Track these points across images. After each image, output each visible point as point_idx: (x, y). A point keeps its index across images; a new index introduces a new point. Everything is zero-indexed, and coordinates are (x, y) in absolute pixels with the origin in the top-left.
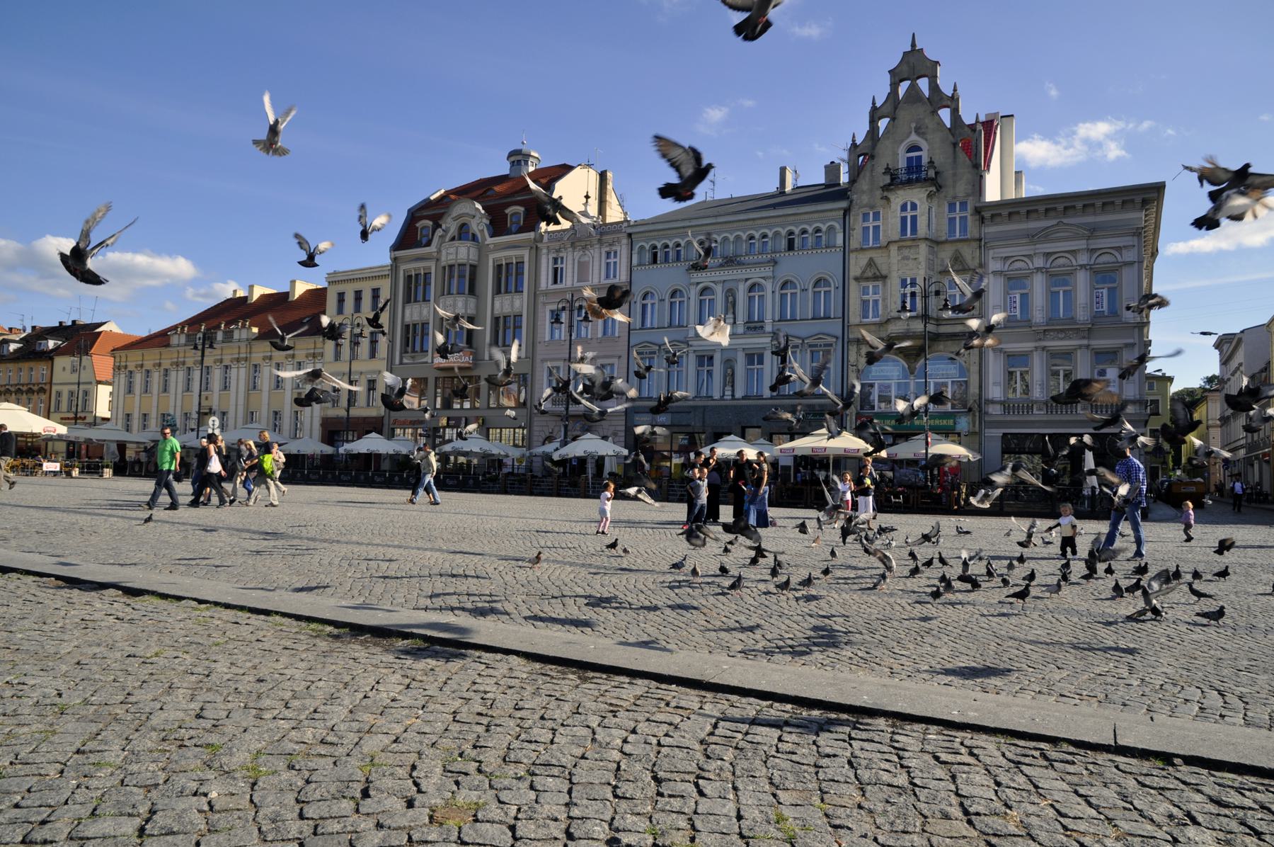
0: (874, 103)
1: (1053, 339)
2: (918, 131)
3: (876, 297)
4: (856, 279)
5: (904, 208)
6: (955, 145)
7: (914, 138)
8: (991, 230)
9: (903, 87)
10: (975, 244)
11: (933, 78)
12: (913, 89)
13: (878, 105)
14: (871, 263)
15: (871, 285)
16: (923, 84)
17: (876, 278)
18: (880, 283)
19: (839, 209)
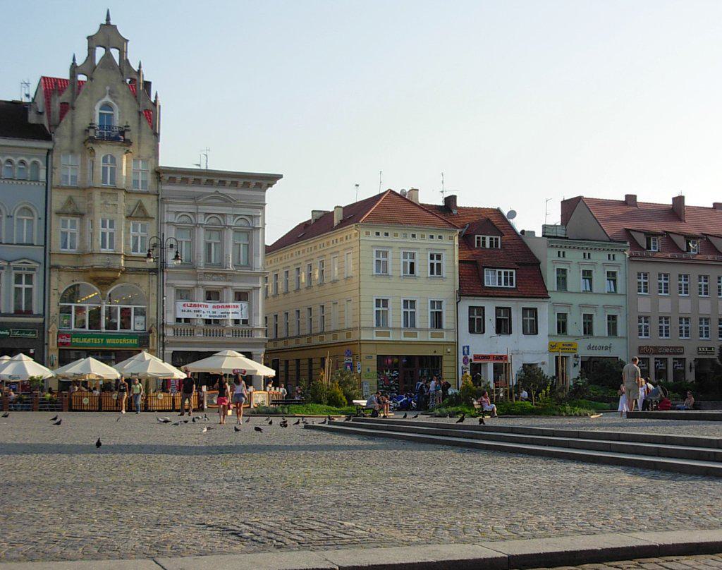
0: (74, 59)
1: (210, 280)
2: (111, 93)
3: (73, 230)
4: (56, 213)
5: (105, 160)
6: (140, 113)
7: (107, 99)
8: (166, 188)
9: (100, 52)
10: (155, 198)
11: (123, 53)
12: (108, 55)
13: (79, 62)
14: (70, 201)
15: (69, 220)
16: (115, 53)
17: (75, 214)
18: (77, 220)
19: (45, 149)
